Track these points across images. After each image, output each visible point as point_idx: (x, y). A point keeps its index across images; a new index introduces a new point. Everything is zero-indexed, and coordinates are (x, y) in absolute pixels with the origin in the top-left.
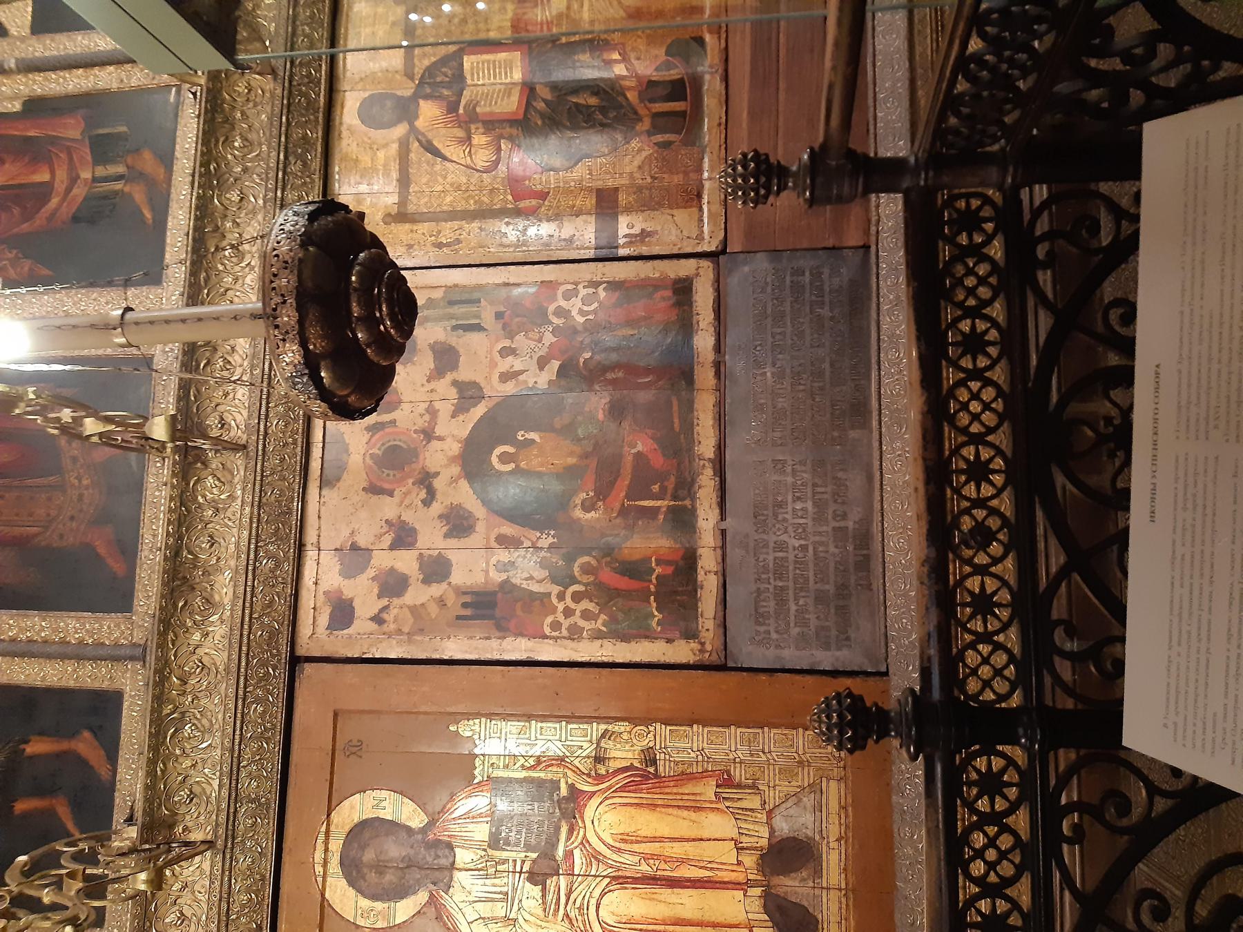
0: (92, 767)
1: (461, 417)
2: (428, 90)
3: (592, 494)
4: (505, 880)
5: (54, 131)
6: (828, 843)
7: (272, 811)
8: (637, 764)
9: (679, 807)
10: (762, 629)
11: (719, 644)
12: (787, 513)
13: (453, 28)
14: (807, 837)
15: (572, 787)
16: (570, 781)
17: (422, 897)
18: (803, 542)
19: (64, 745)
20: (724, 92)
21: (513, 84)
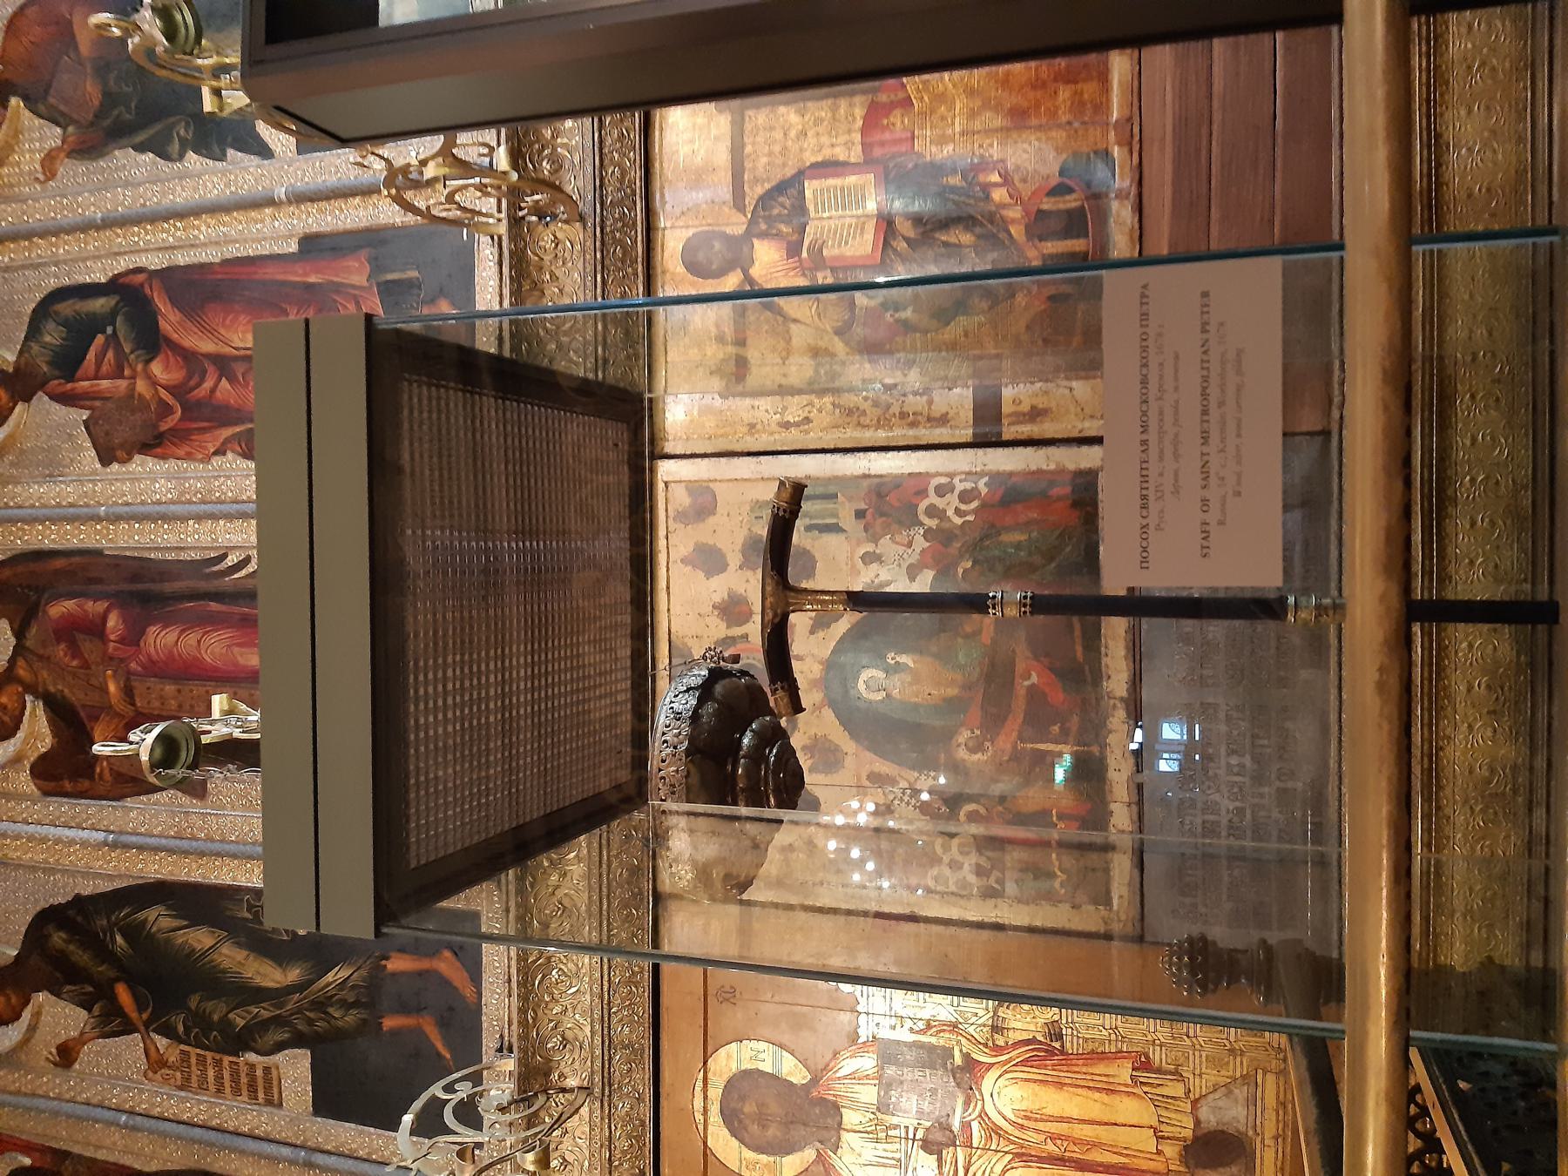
0: (456, 989)
1: (821, 634)
2: (763, 227)
3: (978, 732)
4: (898, 1146)
5: (337, 276)
6: (1263, 1139)
7: (646, 1056)
8: (1040, 1038)
9: (1089, 1088)
10: (1188, 900)
11: (1134, 912)
12: (1219, 768)
13: (790, 143)
14: (1238, 1131)
15: (967, 1057)
16: (964, 1050)
17: (809, 1154)
18: (1238, 804)
19: (424, 964)
20: (1137, 226)
21: (867, 216)
